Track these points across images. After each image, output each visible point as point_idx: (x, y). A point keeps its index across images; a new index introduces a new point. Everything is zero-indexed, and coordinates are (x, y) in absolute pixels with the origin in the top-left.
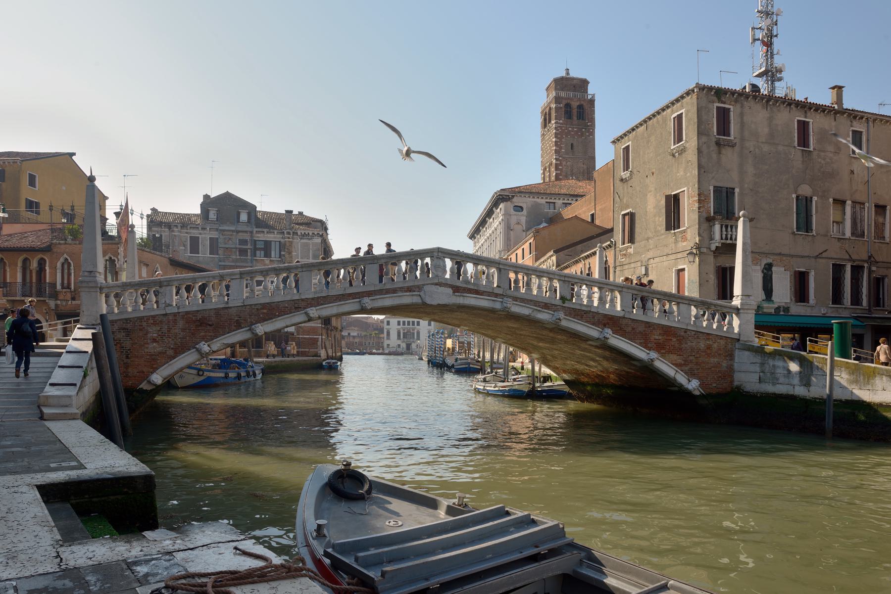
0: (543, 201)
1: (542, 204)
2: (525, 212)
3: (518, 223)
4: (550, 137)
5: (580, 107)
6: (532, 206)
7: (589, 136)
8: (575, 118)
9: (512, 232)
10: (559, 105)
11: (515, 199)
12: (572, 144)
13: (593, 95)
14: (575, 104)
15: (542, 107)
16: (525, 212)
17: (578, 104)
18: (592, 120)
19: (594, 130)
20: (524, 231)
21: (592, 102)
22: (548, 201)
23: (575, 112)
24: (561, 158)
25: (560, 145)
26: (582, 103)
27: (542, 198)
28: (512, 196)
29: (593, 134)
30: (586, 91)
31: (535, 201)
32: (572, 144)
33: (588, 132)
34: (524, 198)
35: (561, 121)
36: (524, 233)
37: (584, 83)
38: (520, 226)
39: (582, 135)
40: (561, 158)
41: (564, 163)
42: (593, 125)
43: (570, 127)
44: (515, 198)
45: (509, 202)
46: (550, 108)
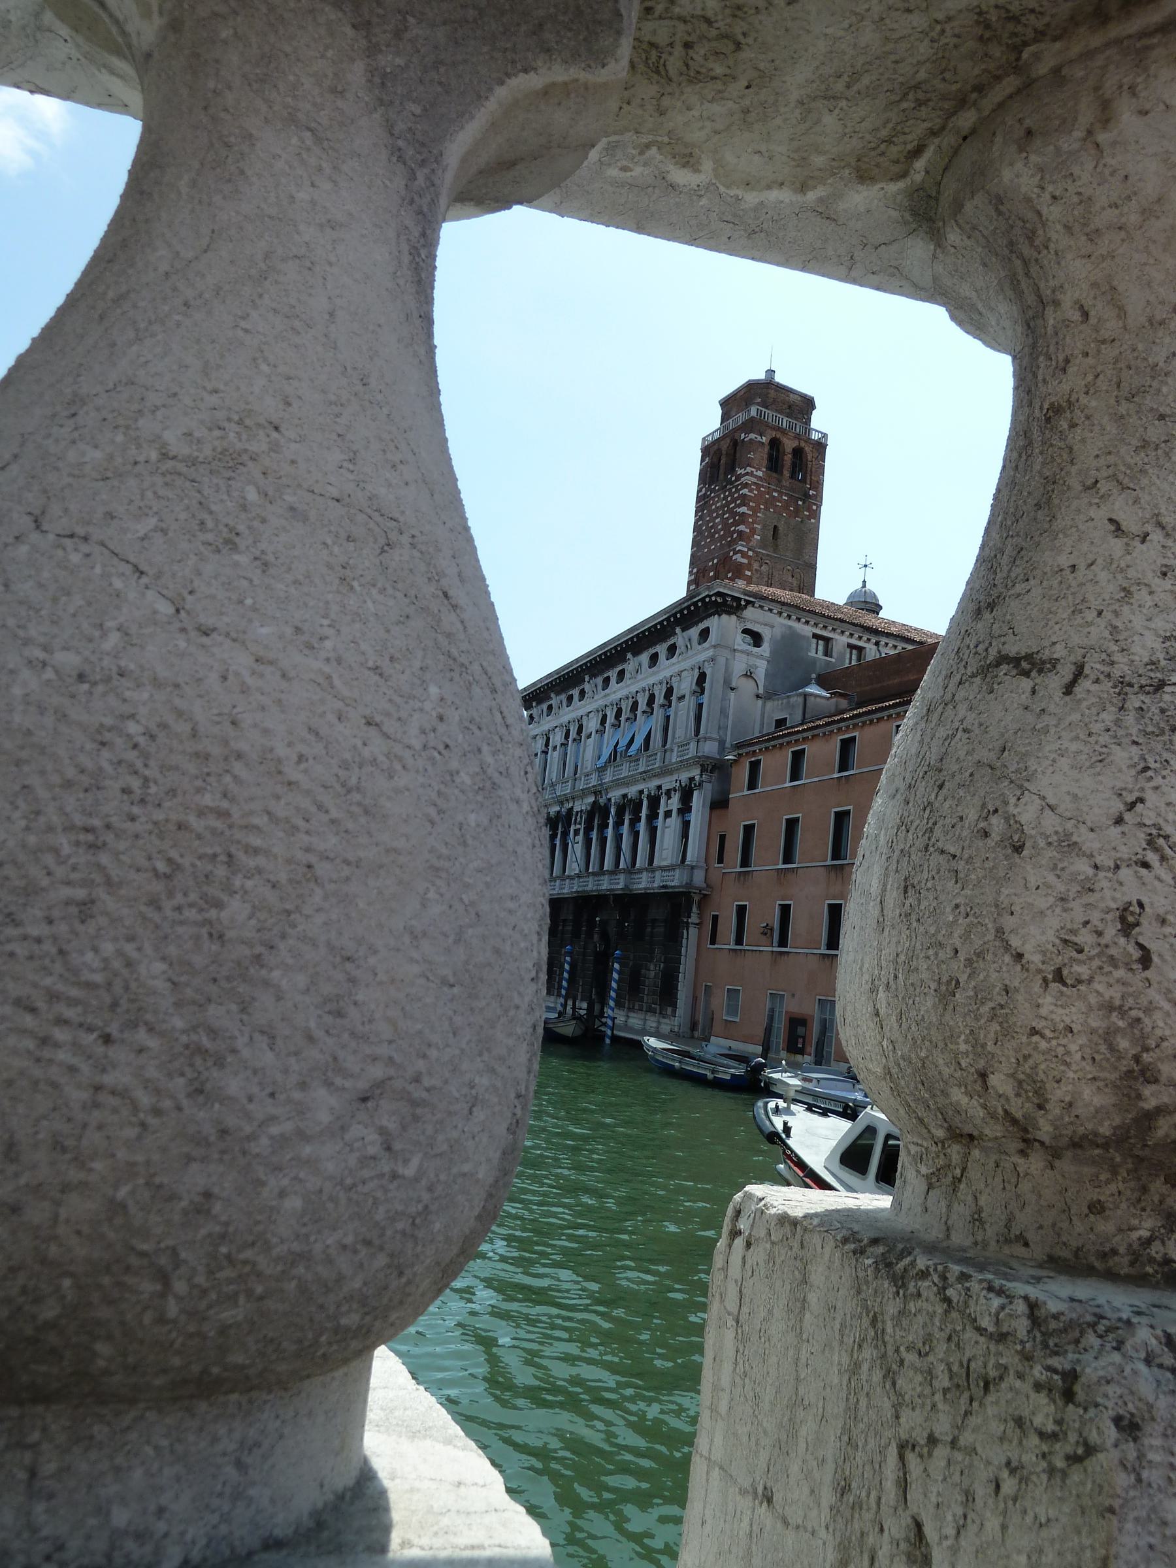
0: (808, 630)
1: (804, 637)
2: (765, 649)
3: (749, 675)
4: (728, 504)
5: (798, 452)
6: (783, 637)
7: (809, 517)
8: (787, 474)
9: (732, 695)
10: (759, 438)
11: (749, 612)
12: (775, 527)
13: (825, 436)
14: (789, 444)
15: (704, 439)
16: (765, 649)
17: (795, 444)
18: (818, 486)
19: (819, 507)
20: (758, 696)
21: (820, 447)
22: (818, 631)
23: (788, 458)
24: (750, 553)
25: (753, 523)
26: (803, 444)
27: (807, 622)
28: (748, 602)
29: (816, 515)
30: (808, 422)
31: (790, 627)
32: (775, 527)
33: (809, 509)
34: (769, 613)
35: (760, 474)
36: (760, 702)
37: (808, 404)
38: (751, 683)
39: (797, 512)
40: (750, 553)
41: (756, 566)
42: (819, 498)
43: (775, 491)
44: (750, 608)
45: (734, 618)
46: (719, 450)
